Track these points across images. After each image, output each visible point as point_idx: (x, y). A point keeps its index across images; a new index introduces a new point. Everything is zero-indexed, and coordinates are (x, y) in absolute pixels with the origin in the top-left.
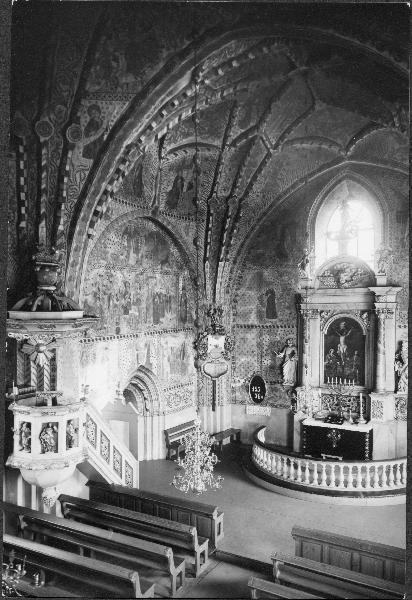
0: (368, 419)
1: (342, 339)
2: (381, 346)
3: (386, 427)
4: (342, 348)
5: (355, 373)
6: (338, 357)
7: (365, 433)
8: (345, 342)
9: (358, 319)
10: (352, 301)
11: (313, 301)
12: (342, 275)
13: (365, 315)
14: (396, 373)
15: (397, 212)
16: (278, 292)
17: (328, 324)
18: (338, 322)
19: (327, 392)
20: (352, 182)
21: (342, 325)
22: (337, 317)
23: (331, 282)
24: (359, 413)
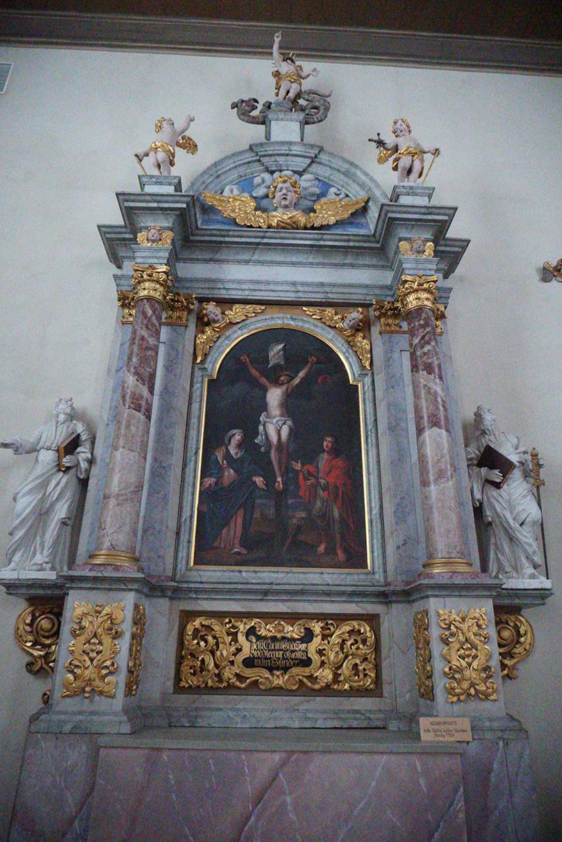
1: (274, 396)
4: (275, 426)
5: (325, 515)
6: (255, 454)
8: (288, 406)
14: (478, 511)
18: (257, 343)
21: (276, 352)
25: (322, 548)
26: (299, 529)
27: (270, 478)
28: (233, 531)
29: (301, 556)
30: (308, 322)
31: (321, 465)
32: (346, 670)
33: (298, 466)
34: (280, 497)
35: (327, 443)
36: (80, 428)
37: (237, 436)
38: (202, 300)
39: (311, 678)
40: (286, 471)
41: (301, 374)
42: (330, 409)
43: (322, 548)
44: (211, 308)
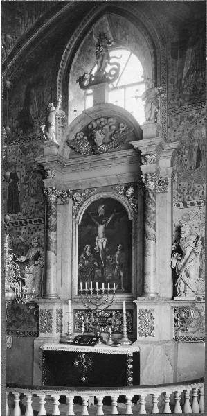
0: (133, 339)
1: (101, 229)
2: (150, 230)
3: (159, 343)
4: (101, 242)
7: (125, 357)
8: (106, 234)
9: (121, 199)
10: (110, 173)
11: (56, 178)
12: (98, 133)
13: (130, 191)
14: (174, 271)
15: (173, 44)
16: (21, 175)
17: (83, 210)
19: (82, 307)
20: (113, 16)
21: (101, 209)
22: (94, 198)
23: (85, 147)
24: (122, 333)
27: (99, 261)
30: (113, 195)
33: (109, 257)
34: (103, 269)
35: (119, 247)
37: (88, 247)
40: (105, 259)
41: (110, 218)
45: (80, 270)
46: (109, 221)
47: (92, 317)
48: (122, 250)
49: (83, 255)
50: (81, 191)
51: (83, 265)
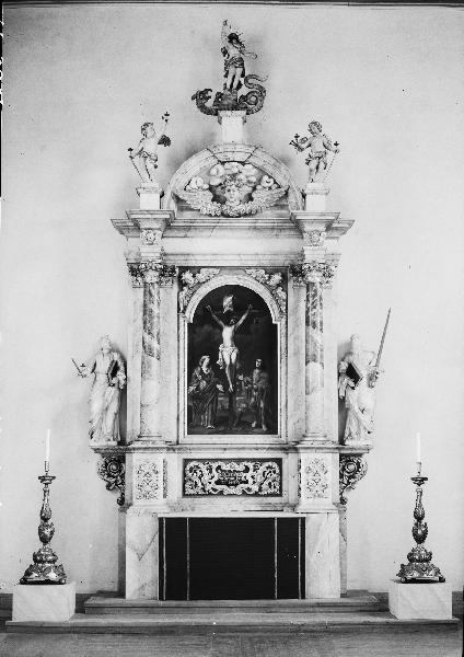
1: (227, 333)
4: (228, 353)
5: (256, 406)
6: (217, 371)
8: (236, 340)
14: (342, 401)
18: (216, 296)
21: (228, 301)
25: (254, 425)
26: (242, 414)
27: (226, 386)
28: (207, 416)
29: (243, 427)
31: (255, 376)
32: (265, 486)
33: (241, 378)
34: (231, 396)
36: (116, 357)
37: (206, 359)
38: (184, 269)
39: (249, 489)
40: (235, 380)
41: (244, 317)
42: (261, 344)
43: (254, 425)
44: (187, 276)
45: (191, 397)
46: (240, 322)
47: (214, 471)
48: (262, 368)
49: (196, 372)
50: (196, 270)
51: (198, 386)
